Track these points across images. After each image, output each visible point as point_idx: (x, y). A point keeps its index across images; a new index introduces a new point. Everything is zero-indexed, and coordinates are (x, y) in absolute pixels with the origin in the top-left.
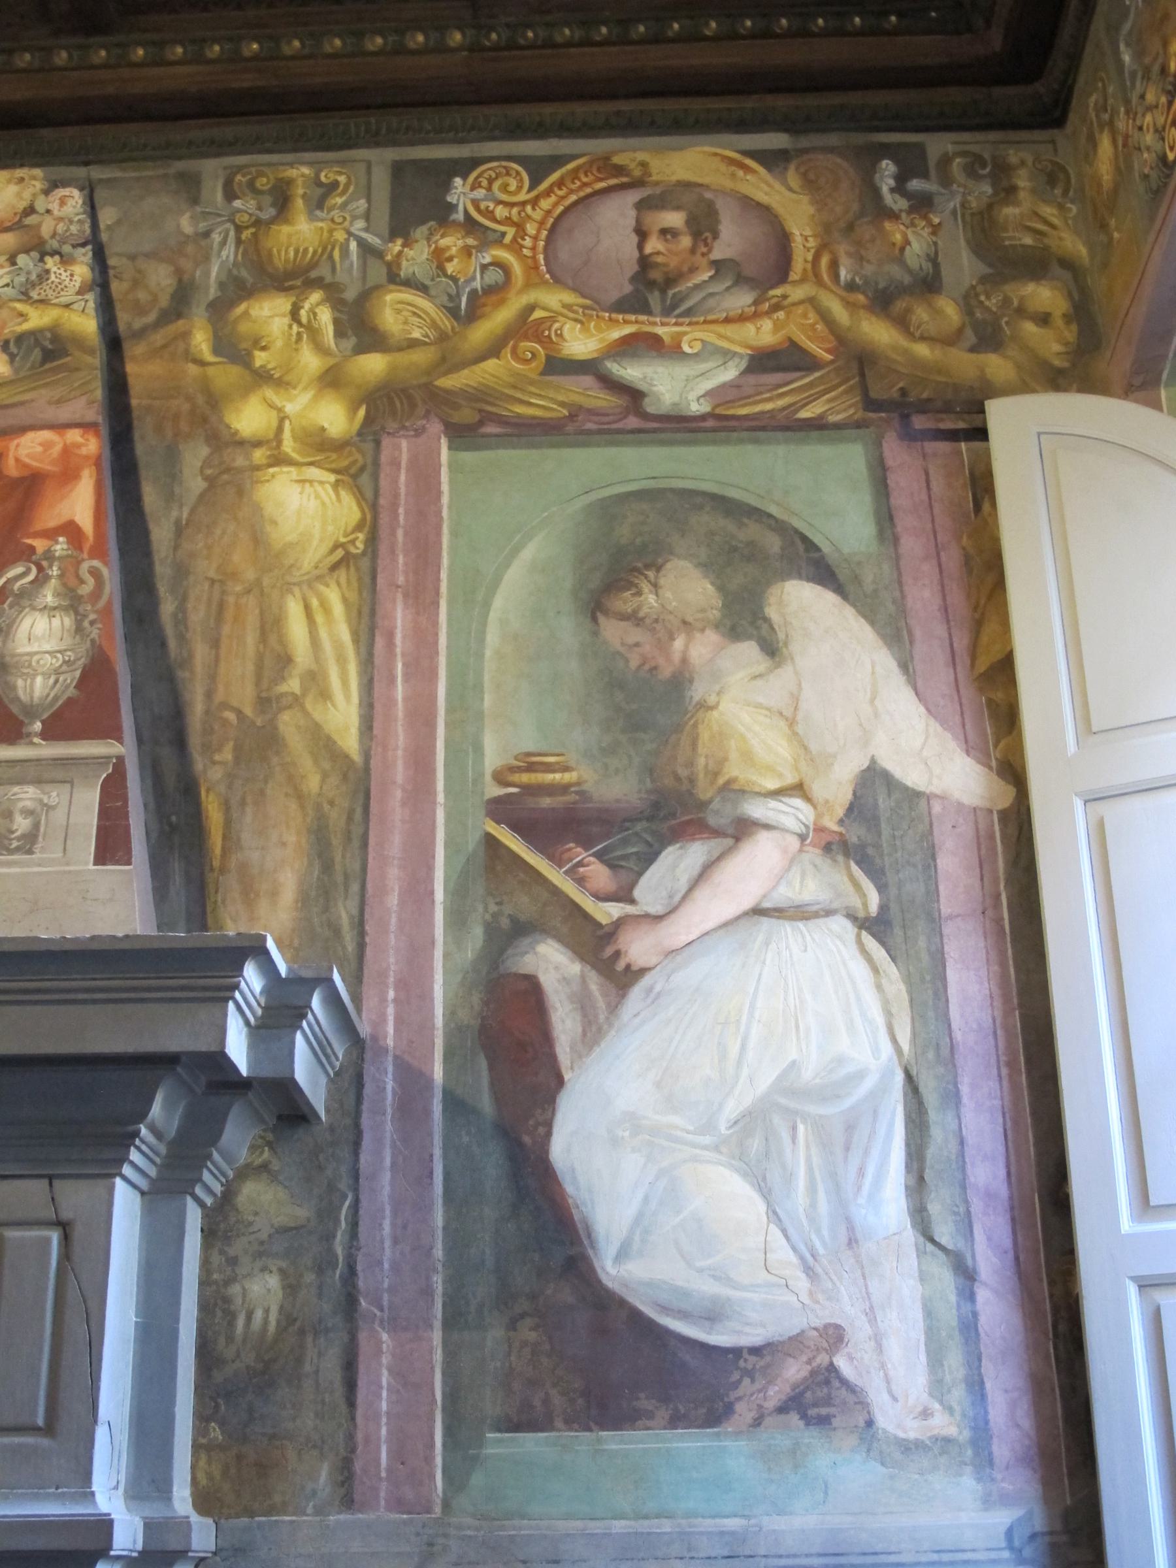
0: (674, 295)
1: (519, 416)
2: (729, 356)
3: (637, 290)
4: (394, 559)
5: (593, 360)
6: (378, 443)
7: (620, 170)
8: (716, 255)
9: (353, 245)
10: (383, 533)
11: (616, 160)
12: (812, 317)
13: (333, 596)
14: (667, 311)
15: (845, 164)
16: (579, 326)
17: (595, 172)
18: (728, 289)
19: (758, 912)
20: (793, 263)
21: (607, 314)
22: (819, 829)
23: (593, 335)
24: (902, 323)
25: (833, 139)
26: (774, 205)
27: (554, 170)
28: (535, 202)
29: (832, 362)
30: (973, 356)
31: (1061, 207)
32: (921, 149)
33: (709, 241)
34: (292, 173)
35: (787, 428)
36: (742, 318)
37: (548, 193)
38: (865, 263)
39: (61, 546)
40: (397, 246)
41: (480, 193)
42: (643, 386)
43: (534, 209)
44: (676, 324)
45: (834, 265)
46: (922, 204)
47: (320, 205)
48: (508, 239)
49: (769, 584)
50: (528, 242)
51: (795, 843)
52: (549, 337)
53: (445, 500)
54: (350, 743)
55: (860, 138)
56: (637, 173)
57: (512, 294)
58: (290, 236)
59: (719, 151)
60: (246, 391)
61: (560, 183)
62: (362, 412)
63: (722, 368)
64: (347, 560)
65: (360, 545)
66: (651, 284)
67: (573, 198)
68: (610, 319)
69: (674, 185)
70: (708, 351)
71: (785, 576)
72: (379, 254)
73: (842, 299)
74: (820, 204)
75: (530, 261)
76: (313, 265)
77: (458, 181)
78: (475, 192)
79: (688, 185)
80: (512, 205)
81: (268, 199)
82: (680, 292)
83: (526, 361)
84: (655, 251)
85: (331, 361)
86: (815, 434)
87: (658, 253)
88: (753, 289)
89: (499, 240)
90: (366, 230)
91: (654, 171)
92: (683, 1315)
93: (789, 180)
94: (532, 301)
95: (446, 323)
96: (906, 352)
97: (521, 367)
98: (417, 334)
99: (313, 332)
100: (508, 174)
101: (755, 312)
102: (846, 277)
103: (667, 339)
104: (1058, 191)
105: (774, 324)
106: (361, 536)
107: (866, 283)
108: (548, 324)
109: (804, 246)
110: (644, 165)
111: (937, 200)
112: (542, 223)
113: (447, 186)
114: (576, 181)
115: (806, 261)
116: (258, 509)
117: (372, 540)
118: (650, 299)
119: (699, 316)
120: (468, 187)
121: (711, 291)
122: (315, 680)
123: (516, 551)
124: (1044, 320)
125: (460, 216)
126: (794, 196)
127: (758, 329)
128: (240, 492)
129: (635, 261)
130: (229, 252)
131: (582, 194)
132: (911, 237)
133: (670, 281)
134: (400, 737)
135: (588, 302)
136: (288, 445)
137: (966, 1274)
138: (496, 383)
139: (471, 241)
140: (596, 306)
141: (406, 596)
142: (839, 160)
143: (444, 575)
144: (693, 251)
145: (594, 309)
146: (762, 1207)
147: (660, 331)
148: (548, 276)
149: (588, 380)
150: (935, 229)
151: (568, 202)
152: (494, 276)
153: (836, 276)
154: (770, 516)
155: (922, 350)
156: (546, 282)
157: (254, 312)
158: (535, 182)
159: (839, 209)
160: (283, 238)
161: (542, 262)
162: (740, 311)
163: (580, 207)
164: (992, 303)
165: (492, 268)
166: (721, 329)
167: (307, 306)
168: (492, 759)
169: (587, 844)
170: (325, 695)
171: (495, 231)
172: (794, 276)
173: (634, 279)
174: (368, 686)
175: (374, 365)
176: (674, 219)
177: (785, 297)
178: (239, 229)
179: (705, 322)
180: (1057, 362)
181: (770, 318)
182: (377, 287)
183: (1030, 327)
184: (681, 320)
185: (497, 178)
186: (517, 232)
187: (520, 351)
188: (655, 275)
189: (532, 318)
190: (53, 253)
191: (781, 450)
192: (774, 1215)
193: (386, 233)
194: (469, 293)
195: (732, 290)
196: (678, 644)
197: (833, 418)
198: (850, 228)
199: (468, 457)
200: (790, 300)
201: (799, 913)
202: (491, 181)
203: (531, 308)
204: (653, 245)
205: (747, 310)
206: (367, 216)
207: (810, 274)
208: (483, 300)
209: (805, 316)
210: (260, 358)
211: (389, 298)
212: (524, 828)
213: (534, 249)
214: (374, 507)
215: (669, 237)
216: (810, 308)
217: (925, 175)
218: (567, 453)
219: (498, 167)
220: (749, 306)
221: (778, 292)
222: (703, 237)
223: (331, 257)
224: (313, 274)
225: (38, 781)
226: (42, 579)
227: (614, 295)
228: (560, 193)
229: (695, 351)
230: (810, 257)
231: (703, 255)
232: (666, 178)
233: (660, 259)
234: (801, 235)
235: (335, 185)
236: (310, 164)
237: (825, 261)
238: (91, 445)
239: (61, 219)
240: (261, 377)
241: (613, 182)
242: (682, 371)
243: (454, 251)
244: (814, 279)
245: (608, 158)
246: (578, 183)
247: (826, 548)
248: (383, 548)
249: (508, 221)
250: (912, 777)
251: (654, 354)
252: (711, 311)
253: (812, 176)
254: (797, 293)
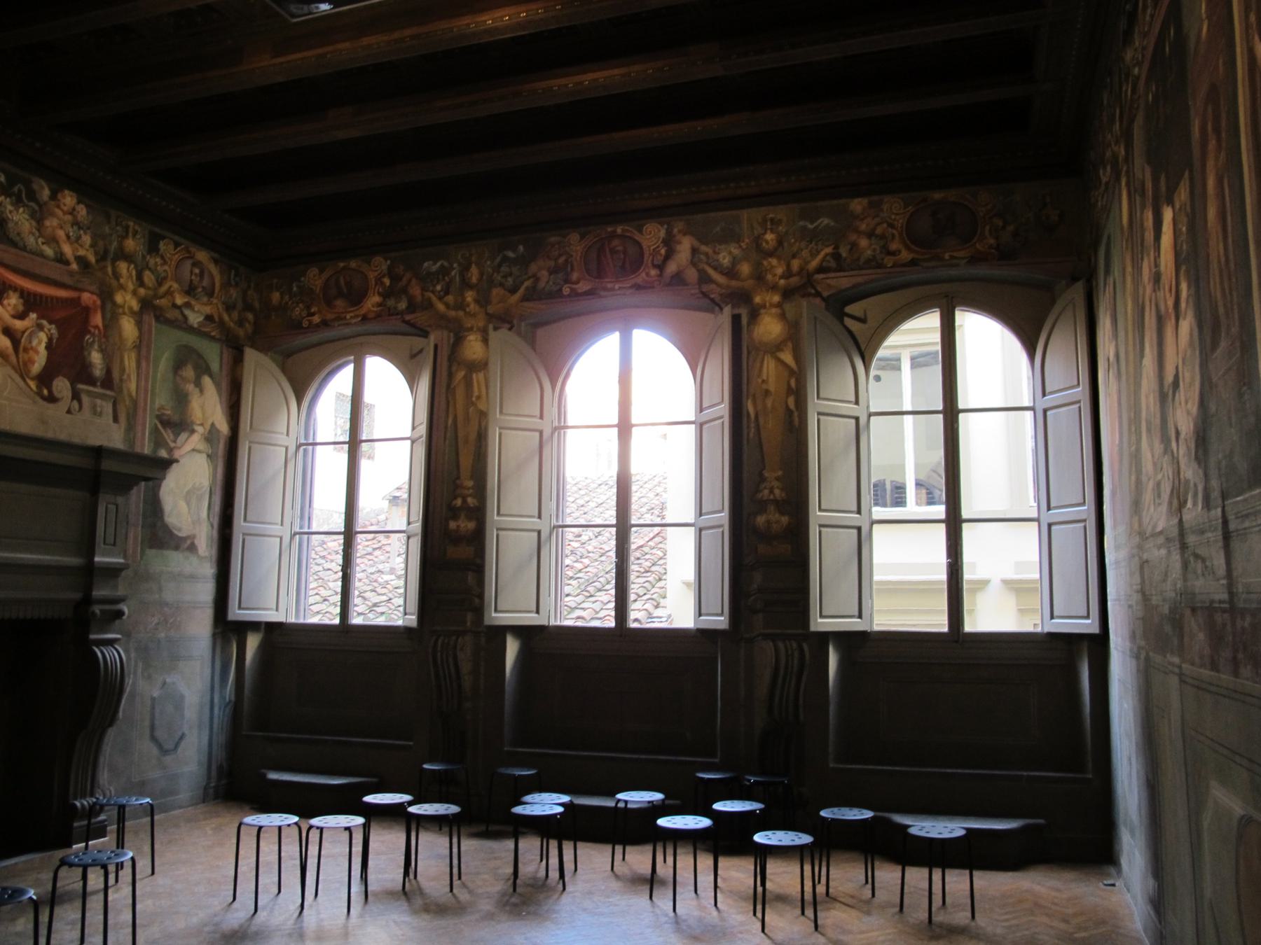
19: (193, 450)
22: (204, 434)
24: (230, 316)
37: (176, 253)
39: (97, 332)
40: (148, 257)
41: (165, 247)
46: (237, 285)
51: (200, 436)
54: (134, 394)
62: (140, 305)
64: (134, 347)
77: (161, 242)
92: (176, 530)
99: (131, 276)
106: (138, 341)
117: (140, 342)
122: (129, 376)
124: (249, 323)
130: (115, 243)
134: (142, 396)
136: (126, 310)
137: (212, 526)
146: (187, 509)
168: (157, 405)
169: (170, 429)
170: (130, 380)
172: (215, 295)
174: (137, 382)
175: (142, 291)
176: (197, 271)
178: (119, 236)
190: (82, 229)
192: (189, 512)
196: (187, 386)
201: (199, 451)
203: (171, 287)
204: (193, 277)
210: (122, 281)
212: (162, 422)
225: (101, 399)
226: (94, 341)
238: (99, 302)
239: (82, 216)
250: (218, 426)
254: (215, 301)
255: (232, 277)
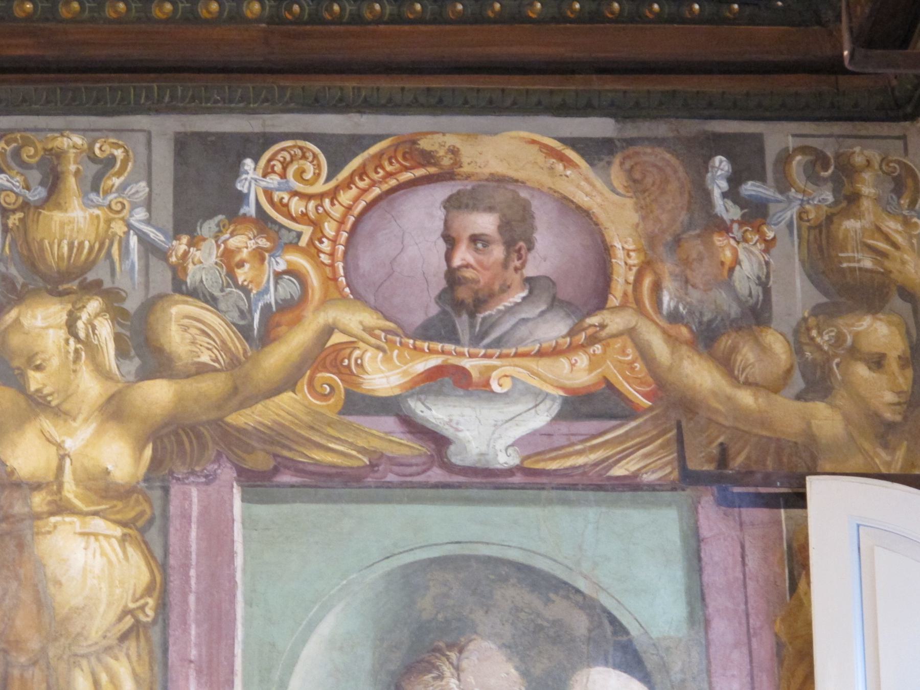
0: (484, 319)
1: (317, 463)
2: (540, 399)
3: (444, 312)
4: (186, 631)
5: (396, 397)
6: (166, 490)
7: (428, 158)
8: (530, 271)
9: (134, 240)
10: (174, 598)
11: (425, 144)
12: (631, 353)
13: (123, 670)
14: (476, 340)
15: (674, 161)
16: (381, 355)
17: (400, 159)
18: (542, 313)
20: (613, 285)
21: (411, 341)
23: (398, 367)
24: (726, 364)
25: (662, 129)
26: (596, 210)
27: (355, 155)
28: (333, 195)
29: (650, 409)
30: (799, 404)
31: (906, 222)
32: (758, 138)
33: (523, 252)
34: (63, 142)
35: (599, 488)
36: (555, 352)
37: (348, 184)
38: (690, 287)
40: (182, 245)
41: (273, 180)
42: (448, 432)
43: (332, 204)
44: (485, 356)
45: (657, 288)
47: (95, 188)
48: (303, 242)
49: (574, 669)
50: (326, 246)
52: (349, 366)
53: (239, 561)
55: (692, 127)
56: (446, 162)
57: (308, 313)
58: (62, 225)
59: (537, 137)
60: (22, 421)
61: (362, 172)
62: (148, 452)
63: (533, 411)
64: (137, 629)
65: (150, 613)
66: (459, 305)
67: (376, 191)
68: (415, 348)
69: (487, 180)
70: (520, 391)
71: (591, 661)
72: (163, 255)
73: (664, 332)
74: (645, 210)
75: (328, 269)
76: (90, 264)
77: (248, 163)
78: (268, 179)
79: (500, 180)
80: (309, 197)
81: (35, 176)
82: (490, 316)
83: (324, 397)
84: (464, 263)
85: (113, 388)
86: (628, 495)
87: (468, 266)
88: (568, 315)
89: (293, 245)
90: (148, 222)
91: (465, 160)
93: (612, 177)
94: (330, 320)
95: (237, 344)
96: (729, 398)
97: (318, 403)
98: (205, 358)
99: (91, 348)
100: (304, 157)
101: (571, 343)
102: (669, 305)
103: (475, 374)
104: (904, 202)
105: (590, 360)
106: (151, 602)
107: (691, 313)
108: (348, 351)
109: (626, 263)
110: (454, 151)
111: (772, 208)
112: (341, 222)
113: (235, 171)
114: (379, 170)
115: (627, 282)
116: (40, 565)
117: (163, 606)
118: (458, 326)
119: (509, 348)
120: (260, 172)
121: (523, 316)
123: (311, 627)
124: (877, 362)
125: (250, 210)
126: (616, 198)
127: (573, 365)
128: (21, 546)
129: (442, 275)
131: (385, 187)
132: (742, 256)
133: (480, 303)
135: (391, 325)
136: (70, 490)
138: (292, 422)
139: (263, 243)
140: (400, 331)
141: (199, 672)
142: (668, 156)
143: (238, 650)
144: (505, 265)
145: (397, 335)
147: (467, 363)
148: (347, 290)
149: (390, 422)
150: (769, 244)
151: (370, 196)
152: (288, 288)
153: (658, 303)
154: (578, 591)
155: (746, 398)
156: (344, 297)
157: (26, 322)
158: (334, 168)
159: (664, 217)
160: (55, 227)
161: (342, 272)
162: (554, 343)
163: (383, 204)
164: (824, 340)
165: (286, 277)
166: (532, 363)
167: (84, 316)
171: (290, 230)
172: (614, 300)
173: (440, 298)
177: (603, 326)
179: (517, 355)
180: (888, 415)
181: (586, 352)
182: (161, 297)
183: (862, 371)
184: (490, 351)
185: (292, 161)
186: (313, 233)
187: (317, 384)
188: (463, 293)
189: (330, 343)
191: (592, 513)
193: (170, 227)
194: (262, 309)
195: (548, 316)
197: (649, 478)
198: (677, 241)
199: (263, 511)
200: (607, 331)
202: (285, 166)
203: (329, 330)
205: (561, 341)
206: (148, 204)
207: (631, 298)
208: (277, 319)
209: (623, 352)
210: (35, 380)
211: (174, 310)
213: (332, 255)
214: (164, 567)
215: (480, 245)
216: (629, 343)
217: (761, 177)
218: (366, 510)
219: (294, 146)
220: (564, 337)
221: (594, 320)
222: (517, 248)
223: (109, 255)
224: (91, 277)
227: (418, 319)
228: (362, 184)
229: (505, 390)
230: (631, 279)
231: (516, 269)
232: (478, 170)
233: (468, 274)
234: (623, 248)
235: (112, 160)
236: (83, 131)
237: (647, 282)
240: (38, 404)
241: (420, 172)
242: (491, 413)
243: (245, 254)
244: (635, 306)
245: (414, 142)
246: (382, 173)
247: (634, 630)
248: (174, 618)
249: (303, 218)
251: (461, 392)
252: (522, 341)
253: (637, 176)
254: (615, 322)
255: (718, 186)
